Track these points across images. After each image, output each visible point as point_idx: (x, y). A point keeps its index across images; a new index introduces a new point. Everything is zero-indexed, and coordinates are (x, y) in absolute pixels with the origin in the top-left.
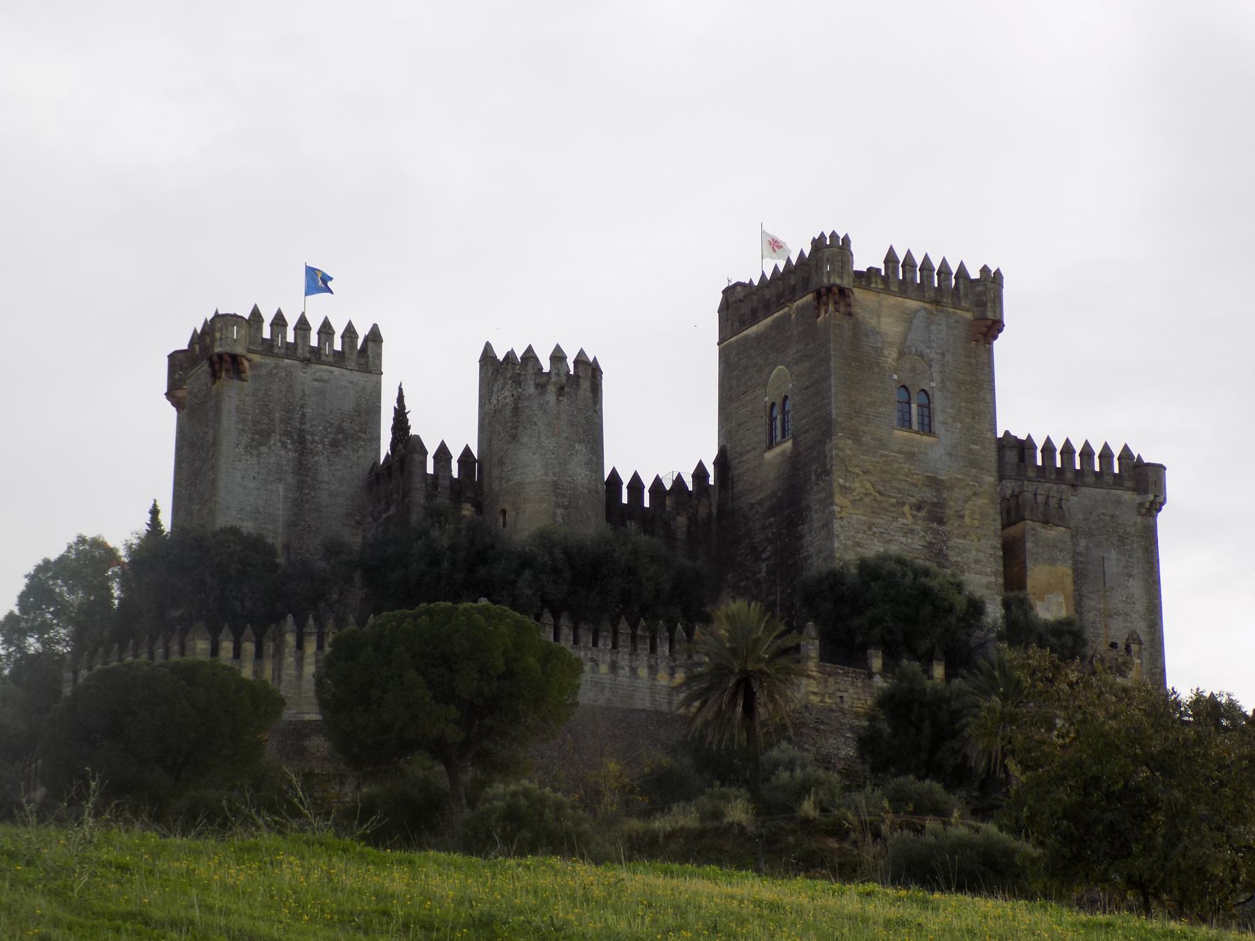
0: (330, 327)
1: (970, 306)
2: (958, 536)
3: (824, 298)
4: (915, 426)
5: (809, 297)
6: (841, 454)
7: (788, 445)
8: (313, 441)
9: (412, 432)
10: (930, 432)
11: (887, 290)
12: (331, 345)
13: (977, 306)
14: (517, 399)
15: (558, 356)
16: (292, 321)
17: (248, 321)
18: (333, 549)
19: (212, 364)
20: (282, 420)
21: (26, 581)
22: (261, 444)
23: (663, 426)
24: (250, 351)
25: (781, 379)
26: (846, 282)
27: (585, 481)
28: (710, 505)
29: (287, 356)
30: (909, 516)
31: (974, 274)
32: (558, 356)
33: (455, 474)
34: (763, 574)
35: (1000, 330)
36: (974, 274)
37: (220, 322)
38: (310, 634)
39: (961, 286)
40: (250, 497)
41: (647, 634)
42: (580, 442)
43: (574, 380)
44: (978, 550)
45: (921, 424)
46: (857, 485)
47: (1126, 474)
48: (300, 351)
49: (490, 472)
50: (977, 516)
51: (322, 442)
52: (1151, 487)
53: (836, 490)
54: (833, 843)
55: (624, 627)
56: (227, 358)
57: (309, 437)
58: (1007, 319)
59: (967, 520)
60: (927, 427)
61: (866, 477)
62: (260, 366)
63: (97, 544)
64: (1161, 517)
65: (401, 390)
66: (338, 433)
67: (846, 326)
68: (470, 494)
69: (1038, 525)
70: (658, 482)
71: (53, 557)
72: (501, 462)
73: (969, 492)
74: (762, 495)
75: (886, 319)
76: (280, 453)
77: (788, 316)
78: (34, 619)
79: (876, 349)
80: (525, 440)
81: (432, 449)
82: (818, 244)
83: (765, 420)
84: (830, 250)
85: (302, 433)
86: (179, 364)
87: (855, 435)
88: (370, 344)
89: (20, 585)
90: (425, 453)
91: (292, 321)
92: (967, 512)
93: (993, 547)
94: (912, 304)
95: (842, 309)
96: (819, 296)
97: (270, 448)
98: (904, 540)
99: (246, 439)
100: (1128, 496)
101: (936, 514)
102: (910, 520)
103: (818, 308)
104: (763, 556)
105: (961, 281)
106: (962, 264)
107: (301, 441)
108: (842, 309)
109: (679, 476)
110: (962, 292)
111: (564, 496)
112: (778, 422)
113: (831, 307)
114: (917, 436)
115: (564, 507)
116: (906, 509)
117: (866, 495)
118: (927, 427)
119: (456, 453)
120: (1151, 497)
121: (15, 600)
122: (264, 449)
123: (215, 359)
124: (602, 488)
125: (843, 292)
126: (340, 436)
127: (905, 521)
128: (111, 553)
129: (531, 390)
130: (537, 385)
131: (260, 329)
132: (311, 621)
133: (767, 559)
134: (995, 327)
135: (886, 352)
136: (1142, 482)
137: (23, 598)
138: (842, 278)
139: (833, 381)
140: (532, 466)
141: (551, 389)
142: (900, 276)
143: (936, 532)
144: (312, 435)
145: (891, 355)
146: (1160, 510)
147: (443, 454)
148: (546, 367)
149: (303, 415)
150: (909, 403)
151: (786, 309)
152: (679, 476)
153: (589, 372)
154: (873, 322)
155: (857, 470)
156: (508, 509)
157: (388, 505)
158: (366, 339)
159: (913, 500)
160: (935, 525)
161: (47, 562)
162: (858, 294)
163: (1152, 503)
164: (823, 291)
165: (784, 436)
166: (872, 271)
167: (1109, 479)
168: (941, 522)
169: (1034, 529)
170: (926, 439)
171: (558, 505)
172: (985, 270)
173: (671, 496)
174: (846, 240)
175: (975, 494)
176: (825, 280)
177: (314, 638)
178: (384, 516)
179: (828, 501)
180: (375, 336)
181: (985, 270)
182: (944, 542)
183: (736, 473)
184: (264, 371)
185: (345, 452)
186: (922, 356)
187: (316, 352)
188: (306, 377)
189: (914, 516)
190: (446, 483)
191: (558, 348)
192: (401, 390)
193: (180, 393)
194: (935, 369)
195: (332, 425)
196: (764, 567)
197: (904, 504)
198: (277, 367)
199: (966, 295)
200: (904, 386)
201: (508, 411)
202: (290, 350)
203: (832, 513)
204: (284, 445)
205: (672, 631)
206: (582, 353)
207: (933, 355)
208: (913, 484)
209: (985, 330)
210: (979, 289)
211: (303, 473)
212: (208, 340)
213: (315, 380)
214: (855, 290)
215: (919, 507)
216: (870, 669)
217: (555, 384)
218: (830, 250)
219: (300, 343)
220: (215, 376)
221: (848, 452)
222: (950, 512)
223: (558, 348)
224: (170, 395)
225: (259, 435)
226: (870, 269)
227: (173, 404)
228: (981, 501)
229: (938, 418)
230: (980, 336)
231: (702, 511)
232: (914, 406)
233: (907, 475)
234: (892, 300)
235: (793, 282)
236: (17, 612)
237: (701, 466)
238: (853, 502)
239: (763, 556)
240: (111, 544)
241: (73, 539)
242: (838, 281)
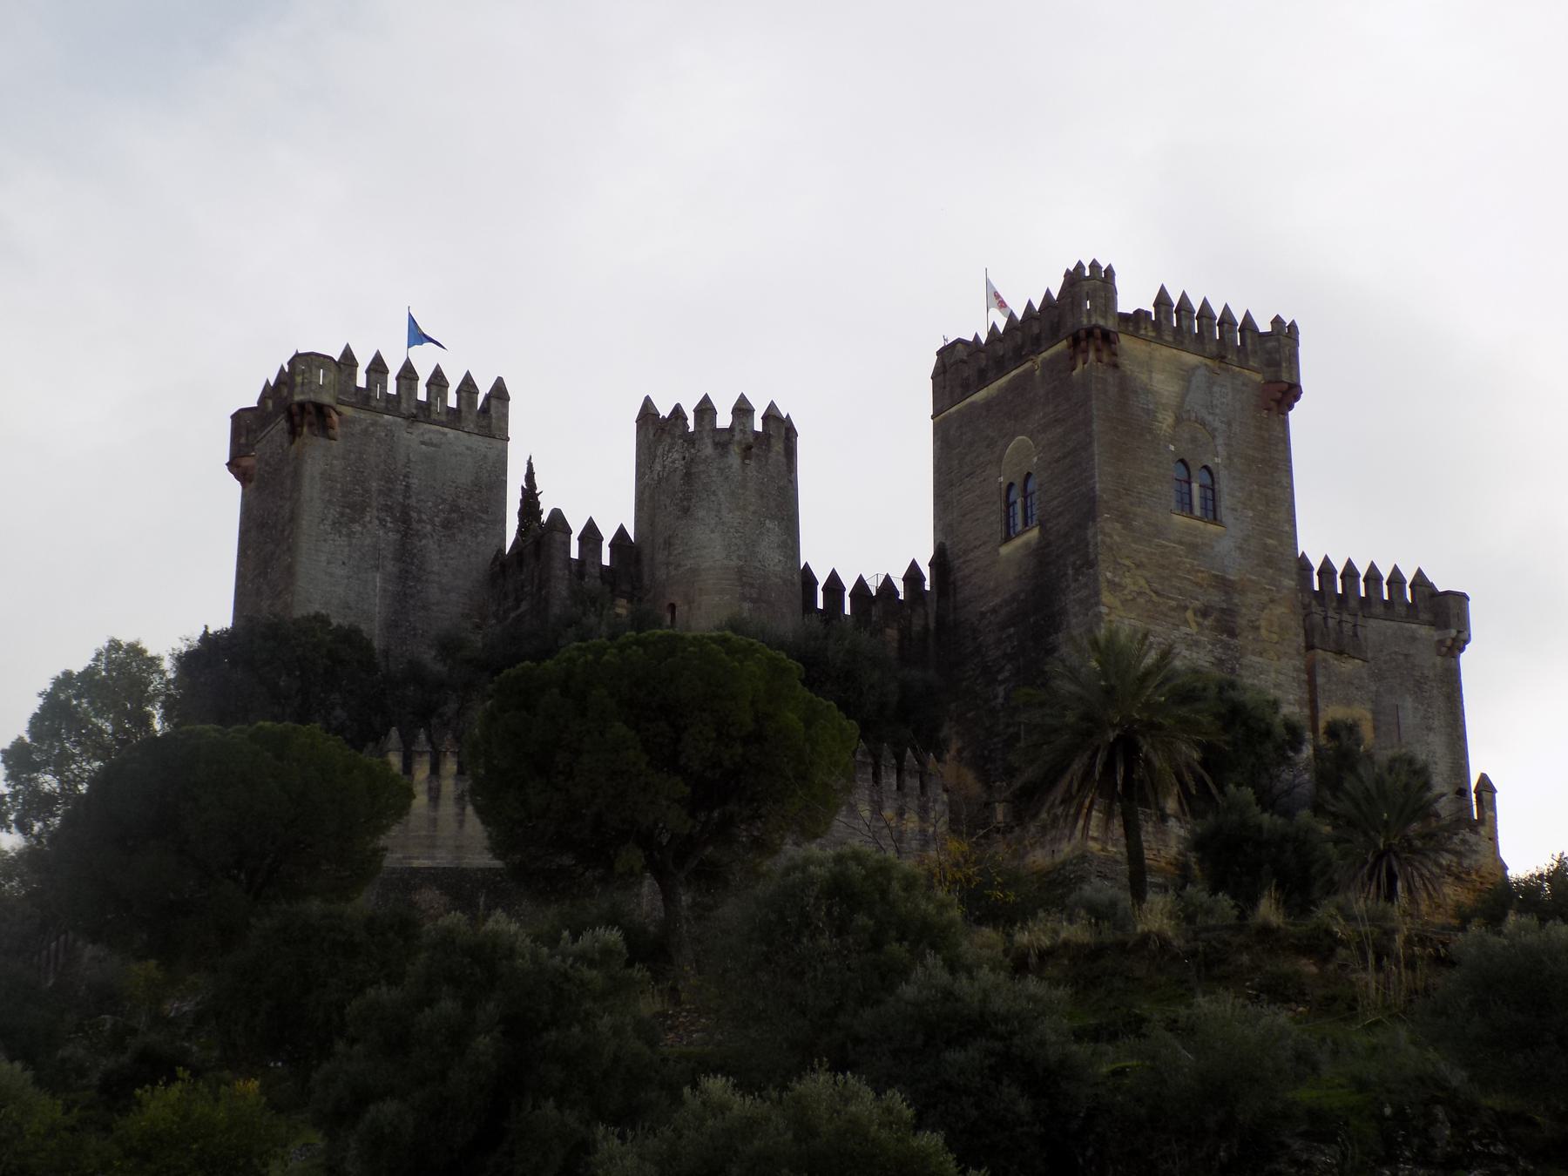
0: (443, 377)
2: (1253, 653)
3: (1083, 344)
4: (1197, 512)
5: (1062, 346)
6: (1108, 540)
7: (1034, 533)
8: (420, 521)
9: (546, 507)
10: (1215, 520)
11: (1159, 339)
12: (444, 400)
13: (1269, 365)
14: (690, 463)
15: (742, 409)
16: (394, 368)
17: (337, 364)
18: (449, 646)
19: (290, 417)
20: (380, 492)
21: (40, 701)
22: (353, 520)
24: (343, 403)
25: (1021, 451)
26: (1111, 324)
27: (779, 568)
28: (927, 615)
30: (1193, 625)
31: (1264, 326)
32: (742, 409)
33: (606, 561)
34: (1000, 700)
35: (1297, 398)
36: (1264, 326)
37: (304, 363)
38: (421, 754)
39: (1249, 341)
40: (337, 582)
41: (870, 760)
42: (773, 518)
43: (763, 439)
44: (1278, 672)
45: (1204, 508)
46: (1128, 581)
47: (1421, 605)
48: (404, 405)
49: (652, 559)
50: (1275, 629)
53: (1104, 585)
54: (1308, 967)
57: (414, 515)
58: (1303, 383)
59: (1263, 632)
61: (1139, 572)
62: (353, 421)
63: (135, 651)
64: (1464, 658)
65: (530, 465)
66: (452, 511)
67: (1110, 379)
68: (625, 587)
69: (1329, 656)
70: (861, 583)
71: (78, 667)
72: (668, 543)
73: (1265, 598)
74: (998, 600)
75: (1160, 374)
78: (52, 746)
79: (1148, 412)
80: (701, 513)
81: (577, 528)
82: (1074, 278)
84: (1089, 285)
85: (406, 510)
86: (245, 426)
87: (1124, 518)
88: (494, 402)
89: (35, 705)
90: (570, 532)
91: (394, 368)
92: (1263, 623)
93: (1297, 670)
94: (1190, 359)
95: (1105, 358)
96: (1076, 341)
97: (364, 526)
98: (1186, 653)
100: (1424, 631)
101: (1226, 623)
102: (1194, 629)
103: (1073, 358)
104: (1000, 678)
105: (1248, 334)
106: (1248, 314)
108: (1105, 358)
109: (888, 579)
110: (1249, 347)
111: (752, 586)
112: (1019, 507)
113: (1092, 356)
114: (1200, 524)
115: (752, 601)
116: (1189, 614)
117: (1140, 594)
119: (608, 535)
120: (1453, 632)
121: (26, 726)
122: (357, 528)
123: (295, 409)
124: (797, 579)
125: (1107, 337)
126: (454, 515)
127: (1188, 630)
128: (153, 662)
129: (709, 450)
130: (716, 445)
131: (353, 375)
132: (422, 737)
133: (1003, 682)
134: (1290, 393)
135: (1160, 416)
137: (37, 722)
138: (1105, 317)
139: (1096, 448)
140: (710, 546)
141: (735, 450)
142: (1174, 321)
143: (1226, 647)
144: (420, 512)
145: (1166, 421)
146: (1462, 649)
147: (591, 533)
148: (724, 420)
149: (408, 486)
150: (1189, 483)
152: (888, 579)
153: (781, 431)
154: (1144, 377)
155: (1127, 562)
156: (678, 603)
157: (518, 601)
158: (488, 398)
159: (1197, 604)
160: (1224, 637)
161: (68, 675)
162: (1125, 341)
163: (1454, 640)
164: (1082, 334)
165: (1026, 524)
166: (1140, 314)
167: (1402, 610)
168: (1232, 634)
169: (1325, 660)
170: (1212, 527)
171: (744, 598)
172: (1277, 321)
174: (1110, 272)
175: (1272, 601)
176: (1085, 321)
177: (427, 758)
178: (513, 615)
179: (1092, 600)
180: (499, 393)
181: (1277, 321)
182: (1237, 659)
184: (357, 429)
185: (460, 537)
187: (425, 407)
188: (412, 439)
189: (1199, 624)
190: (595, 571)
191: (742, 399)
192: (530, 465)
193: (246, 462)
194: (1220, 441)
195: (444, 501)
196: (1001, 691)
197: (1186, 608)
198: (374, 424)
199: (1255, 352)
200: (1182, 461)
201: (677, 479)
202: (392, 403)
203: (1099, 616)
204: (382, 522)
205: (900, 757)
206: (772, 406)
207: (1217, 424)
208: (1197, 584)
209: (1279, 395)
210: (1270, 344)
211: (407, 558)
212: (285, 391)
213: (423, 443)
214: (1122, 337)
215: (1204, 613)
216: (1162, 810)
217: (740, 443)
218: (1089, 285)
219: (404, 396)
220: (294, 432)
221: (1117, 538)
222: (1242, 622)
223: (742, 399)
224: (233, 465)
225: (351, 509)
226: (1138, 312)
227: (237, 478)
228: (1280, 610)
229: (1225, 502)
230: (1273, 404)
231: (917, 624)
232: (1195, 487)
233: (1189, 572)
234: (1166, 352)
235: (1036, 330)
236: (27, 739)
237: (914, 566)
238: (1124, 602)
239: (1000, 678)
240: (151, 652)
241: (103, 643)
242: (1101, 322)
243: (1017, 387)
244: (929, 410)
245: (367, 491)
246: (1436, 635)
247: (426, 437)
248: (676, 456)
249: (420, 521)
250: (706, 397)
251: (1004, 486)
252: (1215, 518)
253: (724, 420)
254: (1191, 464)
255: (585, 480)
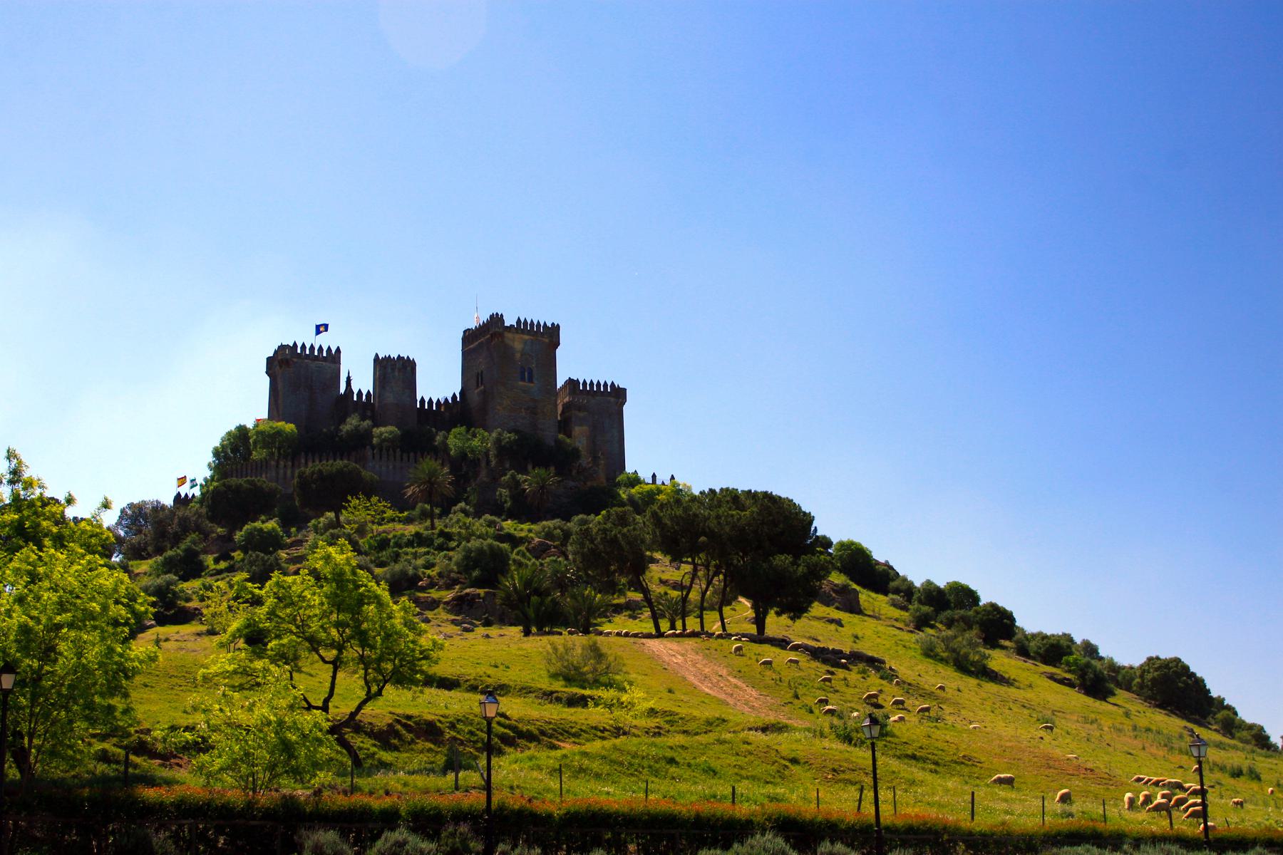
1: (548, 337)
23: (439, 381)
31: (549, 325)
36: (549, 325)
55: (412, 454)
60: (531, 380)
75: (517, 344)
82: (492, 316)
84: (496, 320)
86: (270, 361)
94: (526, 337)
100: (612, 400)
118: (531, 380)
119: (364, 393)
136: (619, 394)
142: (523, 328)
145: (518, 355)
162: (508, 335)
166: (512, 326)
173: (445, 405)
180: (338, 350)
188: (313, 365)
218: (496, 320)
255: (359, 376)
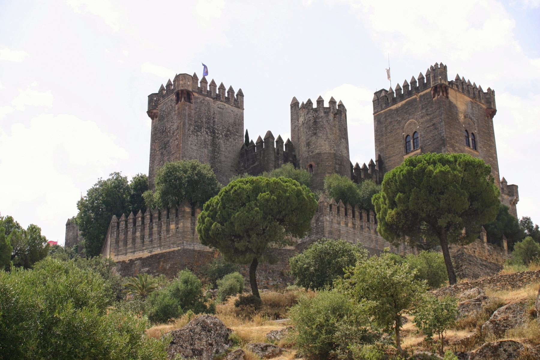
0: (224, 87)
8: (218, 133)
22: (198, 131)
24: (195, 92)
26: (447, 84)
29: (207, 96)
31: (485, 91)
36: (485, 91)
48: (212, 95)
51: (222, 134)
52: (515, 194)
56: (185, 91)
58: (497, 109)
60: (475, 148)
66: (227, 131)
76: (205, 136)
77: (416, 99)
83: (403, 142)
84: (439, 71)
95: (445, 95)
99: (192, 128)
107: (214, 132)
111: (339, 160)
113: (441, 94)
114: (473, 151)
115: (339, 165)
119: (285, 141)
122: (199, 133)
126: (228, 133)
129: (322, 114)
130: (325, 113)
134: (493, 112)
142: (461, 85)
144: (218, 130)
145: (461, 117)
148: (326, 105)
149: (214, 121)
150: (468, 138)
151: (414, 97)
165: (414, 148)
170: (475, 152)
172: (489, 89)
183: (387, 165)
184: (199, 101)
186: (471, 119)
190: (282, 153)
191: (332, 98)
194: (476, 125)
195: (225, 128)
202: (209, 94)
204: (207, 133)
207: (475, 120)
210: (488, 96)
213: (218, 107)
217: (333, 113)
218: (439, 71)
219: (212, 92)
220: (178, 100)
229: (479, 145)
232: (470, 139)
243: (408, 103)
244: (372, 112)
245: (202, 122)
246: (510, 198)
247: (219, 106)
248: (310, 116)
249: (218, 133)
250: (320, 96)
251: (405, 136)
252: (476, 149)
253: (326, 105)
254: (469, 132)
